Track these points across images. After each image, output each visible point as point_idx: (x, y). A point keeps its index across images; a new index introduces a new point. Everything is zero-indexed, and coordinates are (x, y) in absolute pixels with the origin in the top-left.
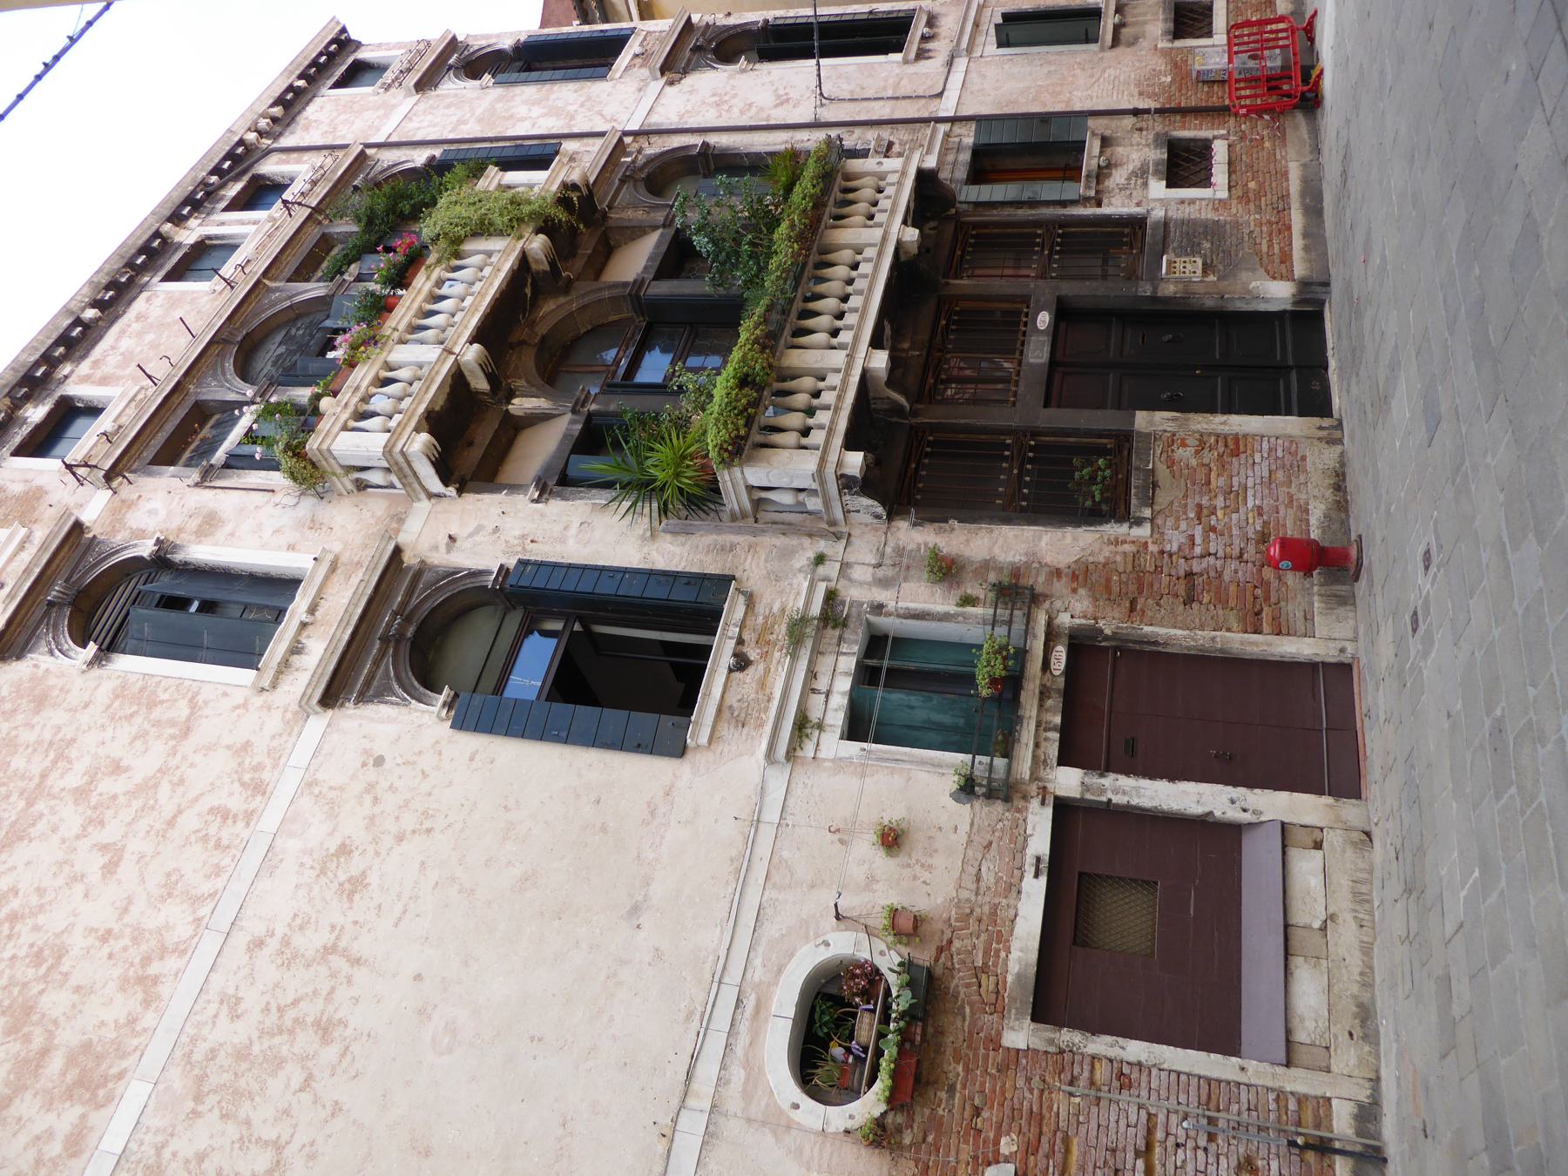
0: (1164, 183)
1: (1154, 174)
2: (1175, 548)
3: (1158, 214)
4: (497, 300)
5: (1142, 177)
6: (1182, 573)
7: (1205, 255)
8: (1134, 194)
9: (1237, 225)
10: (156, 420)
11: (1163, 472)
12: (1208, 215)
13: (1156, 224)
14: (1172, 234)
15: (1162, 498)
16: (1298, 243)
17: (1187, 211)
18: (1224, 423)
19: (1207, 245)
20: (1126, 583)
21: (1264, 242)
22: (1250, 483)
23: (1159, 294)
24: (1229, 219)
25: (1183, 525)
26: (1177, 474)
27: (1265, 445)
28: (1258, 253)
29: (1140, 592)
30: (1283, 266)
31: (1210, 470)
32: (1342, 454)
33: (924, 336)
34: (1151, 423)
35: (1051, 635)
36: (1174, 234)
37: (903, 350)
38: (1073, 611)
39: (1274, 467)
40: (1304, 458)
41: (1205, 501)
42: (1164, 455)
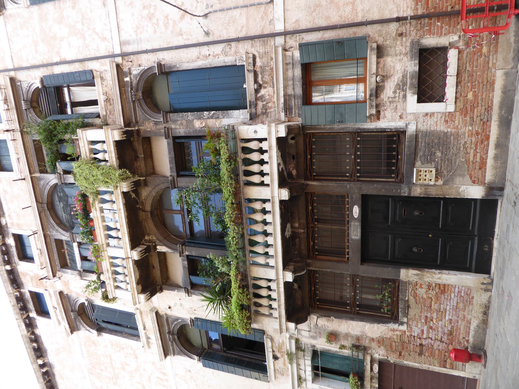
0: (416, 97)
1: (410, 89)
2: (416, 335)
3: (412, 129)
4: (129, 231)
5: (403, 90)
6: (418, 344)
7: (438, 162)
8: (398, 107)
9: (457, 136)
10: (49, 251)
11: (412, 299)
12: (442, 128)
13: (411, 136)
14: (420, 144)
15: (412, 312)
16: (492, 152)
17: (429, 123)
18: (439, 278)
19: (439, 154)
20: (398, 346)
21: (472, 151)
22: (448, 308)
23: (412, 195)
24: (453, 130)
25: (419, 326)
26: (418, 301)
27: (457, 290)
28: (467, 161)
29: (403, 349)
30: (480, 172)
31: (432, 300)
32: (490, 296)
33: (303, 221)
34: (407, 276)
35: (372, 361)
36: (422, 145)
37: (296, 228)
38: (379, 354)
39: (459, 301)
40: (473, 298)
41: (429, 315)
42: (413, 291)
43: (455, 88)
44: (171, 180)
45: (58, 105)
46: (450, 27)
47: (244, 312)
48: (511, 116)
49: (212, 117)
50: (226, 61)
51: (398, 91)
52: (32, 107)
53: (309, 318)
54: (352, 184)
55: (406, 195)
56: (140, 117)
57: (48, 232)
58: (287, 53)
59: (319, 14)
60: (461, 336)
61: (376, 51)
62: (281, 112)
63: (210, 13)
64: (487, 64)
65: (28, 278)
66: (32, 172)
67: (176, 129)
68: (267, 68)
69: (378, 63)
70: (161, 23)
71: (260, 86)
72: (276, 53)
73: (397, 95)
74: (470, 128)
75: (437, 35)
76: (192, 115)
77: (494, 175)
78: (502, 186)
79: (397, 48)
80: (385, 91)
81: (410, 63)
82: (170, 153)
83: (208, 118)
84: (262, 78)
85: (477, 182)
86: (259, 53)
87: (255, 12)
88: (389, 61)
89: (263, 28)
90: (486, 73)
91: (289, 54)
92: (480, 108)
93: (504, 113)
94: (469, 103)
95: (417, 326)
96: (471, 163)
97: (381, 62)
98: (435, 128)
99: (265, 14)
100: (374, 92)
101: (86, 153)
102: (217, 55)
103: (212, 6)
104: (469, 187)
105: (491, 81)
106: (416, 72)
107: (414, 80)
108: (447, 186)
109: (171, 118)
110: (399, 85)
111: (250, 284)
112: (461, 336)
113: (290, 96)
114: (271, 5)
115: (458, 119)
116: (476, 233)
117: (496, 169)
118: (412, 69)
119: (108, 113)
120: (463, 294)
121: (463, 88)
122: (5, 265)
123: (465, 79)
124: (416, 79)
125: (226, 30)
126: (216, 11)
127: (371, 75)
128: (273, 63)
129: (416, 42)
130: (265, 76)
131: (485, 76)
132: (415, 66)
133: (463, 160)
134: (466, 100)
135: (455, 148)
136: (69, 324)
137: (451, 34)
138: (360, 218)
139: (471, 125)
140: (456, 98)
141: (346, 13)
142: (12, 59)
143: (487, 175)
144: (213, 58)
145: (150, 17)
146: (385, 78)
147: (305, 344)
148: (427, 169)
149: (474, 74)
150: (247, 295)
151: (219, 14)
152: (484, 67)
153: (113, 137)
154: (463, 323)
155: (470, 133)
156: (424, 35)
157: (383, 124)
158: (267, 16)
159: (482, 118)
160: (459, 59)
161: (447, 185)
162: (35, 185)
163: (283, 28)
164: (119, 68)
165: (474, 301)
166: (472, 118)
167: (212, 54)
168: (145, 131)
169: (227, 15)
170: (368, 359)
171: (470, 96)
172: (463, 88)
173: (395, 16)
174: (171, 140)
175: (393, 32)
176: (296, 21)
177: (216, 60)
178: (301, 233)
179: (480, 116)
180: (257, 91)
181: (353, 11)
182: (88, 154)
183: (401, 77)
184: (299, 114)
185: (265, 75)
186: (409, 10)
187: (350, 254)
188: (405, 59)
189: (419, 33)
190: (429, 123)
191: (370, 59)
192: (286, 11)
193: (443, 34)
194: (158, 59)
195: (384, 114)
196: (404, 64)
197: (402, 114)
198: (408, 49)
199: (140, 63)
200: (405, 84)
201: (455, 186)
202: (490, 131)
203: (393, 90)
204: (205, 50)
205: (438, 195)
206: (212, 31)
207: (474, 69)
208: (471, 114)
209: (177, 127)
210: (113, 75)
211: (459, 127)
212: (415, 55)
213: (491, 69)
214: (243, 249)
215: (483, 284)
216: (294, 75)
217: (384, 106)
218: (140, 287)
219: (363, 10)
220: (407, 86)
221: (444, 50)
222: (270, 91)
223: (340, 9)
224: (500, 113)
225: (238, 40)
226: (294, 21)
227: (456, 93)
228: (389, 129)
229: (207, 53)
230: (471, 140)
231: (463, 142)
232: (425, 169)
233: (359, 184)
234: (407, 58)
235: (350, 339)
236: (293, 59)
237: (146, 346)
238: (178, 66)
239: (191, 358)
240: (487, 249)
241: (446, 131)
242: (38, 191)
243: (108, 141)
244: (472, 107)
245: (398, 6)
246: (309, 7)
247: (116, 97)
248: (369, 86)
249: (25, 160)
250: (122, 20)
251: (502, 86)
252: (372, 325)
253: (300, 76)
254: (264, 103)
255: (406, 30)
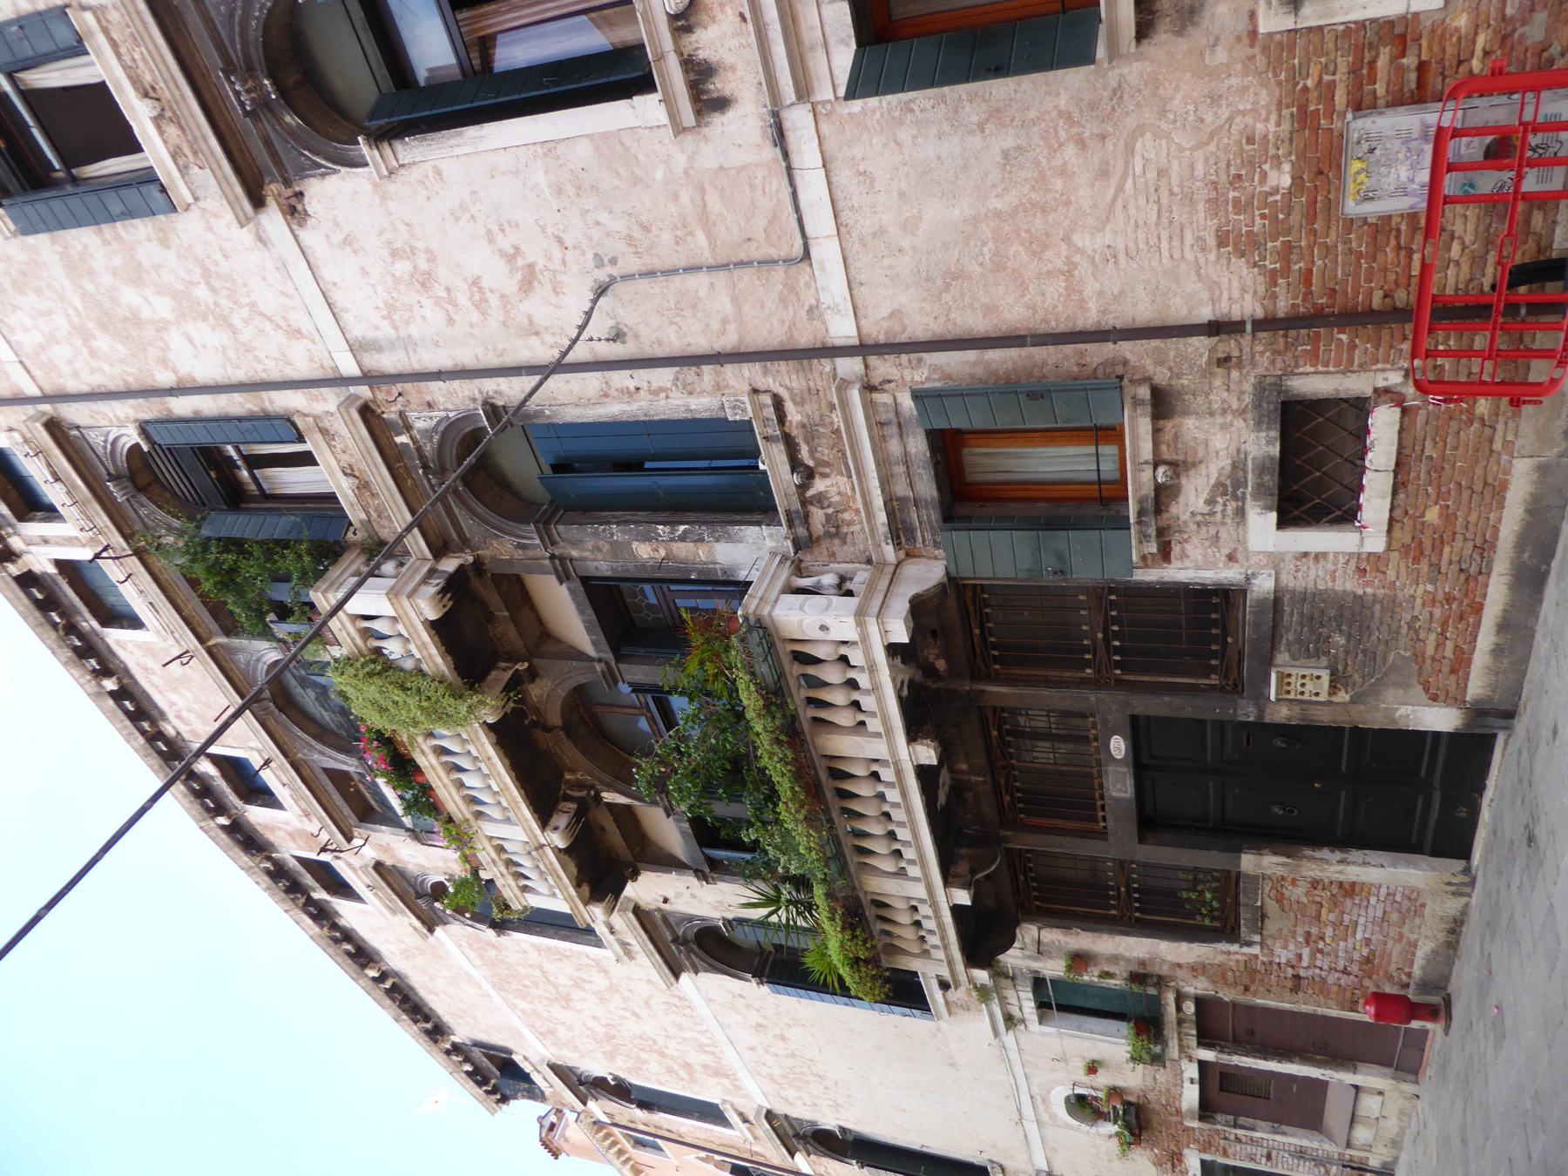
0: (1273, 516)
1: (1256, 497)
2: (1283, 960)
3: (1264, 585)
5: (1235, 497)
6: (1289, 975)
7: (1336, 657)
8: (1223, 535)
9: (1392, 605)
10: (318, 792)
11: (1271, 906)
12: (1348, 584)
13: (1261, 603)
14: (1286, 617)
15: (1271, 926)
16: (1486, 639)
17: (1312, 574)
18: (1340, 872)
19: (1340, 640)
20: (1240, 977)
21: (1433, 637)
22: (1362, 920)
23: (1267, 720)
24: (1380, 592)
25: (1292, 947)
26: (1287, 908)
27: (1383, 891)
28: (1419, 657)
29: (1253, 981)
30: (1453, 678)
31: (1322, 906)
32: (1467, 905)
33: (981, 760)
34: (1259, 866)
35: (1180, 998)
36: (1290, 617)
37: (962, 772)
38: (1197, 987)
39: (1389, 909)
40: (1423, 905)
41: (1314, 931)
42: (1274, 892)
43: (1389, 499)
44: (603, 672)
45: (213, 474)
46: (1377, 346)
47: (863, 969)
48: (1549, 565)
49: (683, 538)
50: (693, 407)
51: (1220, 500)
52: (139, 490)
53: (1018, 931)
54: (1103, 695)
55: (1251, 719)
56: (470, 530)
57: (300, 755)
58: (876, 396)
59: (963, 297)
60: (1393, 967)
61: (1149, 409)
62: (883, 544)
63: (613, 280)
64: (1486, 444)
65: (281, 834)
66: (205, 636)
67: (583, 559)
68: (822, 430)
69: (1156, 432)
70: (463, 300)
71: (809, 475)
72: (845, 405)
73: (1219, 508)
74: (1430, 588)
75: (1338, 364)
76: (624, 532)
77: (1490, 685)
78: (1509, 708)
79: (1212, 397)
80: (1181, 499)
81: (1253, 435)
82: (581, 612)
83: (672, 540)
84: (812, 452)
85: (1442, 697)
86: (790, 390)
87: (758, 283)
88: (1191, 427)
89: (790, 328)
90: (1484, 463)
91: (882, 398)
92: (1458, 543)
93: (1530, 557)
94: (1428, 532)
95: (1285, 947)
96: (1429, 661)
97: (1167, 429)
98: (1330, 584)
99: (791, 287)
100: (1150, 505)
101: (353, 640)
102: (661, 390)
103: (613, 261)
104: (1420, 708)
105: (1496, 484)
106: (1272, 458)
107: (1267, 478)
108: (1362, 707)
109: (564, 535)
110: (1223, 485)
111: (864, 903)
112: (1393, 967)
113: (903, 500)
114: (804, 266)
115: (1396, 568)
116: (1437, 784)
117: (1496, 674)
118: (1262, 452)
119: (374, 515)
120: (1398, 898)
121: (1412, 500)
122: (213, 818)
123: (1418, 478)
124: (1272, 476)
125: (674, 328)
126: (626, 277)
127: (1139, 466)
128: (837, 418)
129: (1270, 384)
130: (819, 449)
131: (1479, 471)
132: (1268, 443)
133: (1408, 654)
134: (1419, 527)
135: (1384, 629)
136: (418, 917)
137: (1379, 366)
138: (1130, 758)
139: (1433, 581)
140: (1391, 521)
141: (1049, 301)
142: (28, 371)
143: (1470, 684)
144: (651, 397)
145: (425, 282)
146: (1178, 467)
147: (1013, 969)
148: (1307, 672)
149: (1447, 467)
150: (865, 941)
151: (643, 285)
152: (1477, 450)
153: (419, 613)
154: (1399, 947)
155: (1428, 598)
156: (1297, 366)
157: (1178, 572)
158: (797, 295)
159: (1464, 566)
160: (1400, 432)
161: (1363, 703)
162: (224, 663)
163: (855, 333)
164: (369, 415)
165: (1427, 911)
166: (1436, 568)
167: (644, 385)
168: (494, 559)
169: (667, 287)
170: (1170, 998)
171: (1432, 515)
172: (1412, 500)
173: (1205, 314)
174: (578, 584)
175: (1201, 356)
176: (892, 315)
177: (663, 403)
178: (977, 782)
179: (1459, 562)
180: (802, 488)
181: (1069, 295)
182: (359, 641)
183: (1229, 468)
184: (935, 542)
185: (818, 445)
186: (1248, 297)
187: (1108, 818)
188: (1239, 423)
189: (1279, 359)
190: (1312, 574)
191: (1132, 429)
192: (854, 286)
193: (1356, 363)
194: (481, 392)
195: (1183, 550)
196: (1235, 436)
197: (1235, 550)
198: (1247, 399)
199: (428, 398)
200: (1239, 483)
201: (1382, 706)
202: (1485, 596)
203: (1204, 496)
204: (621, 378)
205: (1335, 722)
206: (630, 329)
207: (1448, 452)
208: (1434, 559)
209: (587, 554)
210: (360, 442)
211: (1398, 584)
212: (1268, 416)
213: (1500, 454)
214: (839, 856)
215: (1449, 884)
216: (906, 453)
217: (1180, 532)
218: (586, 888)
219: (1101, 294)
220: (1246, 487)
221: (1360, 407)
222: (841, 484)
223: (1027, 289)
224: (1518, 558)
225: (718, 358)
226: (885, 312)
227: (1392, 510)
228: (1198, 584)
229: (631, 384)
230: (1431, 613)
231: (1408, 617)
232: (1302, 672)
233: (1121, 695)
234: (1245, 420)
235: (1122, 963)
236: (897, 414)
237: (625, 958)
238: (547, 412)
239: (740, 979)
240: (1464, 815)
241: (1360, 592)
242: (237, 676)
243: (401, 612)
244: (1438, 542)
245: (1213, 286)
246: (928, 279)
247: (386, 493)
248: (1135, 491)
249: (177, 616)
250: (335, 284)
251: (1527, 497)
252: (1176, 944)
253: (925, 455)
254: (830, 511)
255: (1241, 350)
